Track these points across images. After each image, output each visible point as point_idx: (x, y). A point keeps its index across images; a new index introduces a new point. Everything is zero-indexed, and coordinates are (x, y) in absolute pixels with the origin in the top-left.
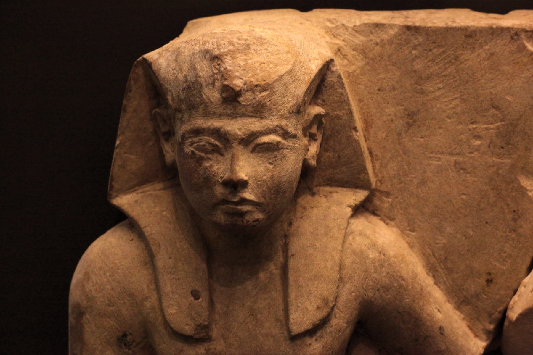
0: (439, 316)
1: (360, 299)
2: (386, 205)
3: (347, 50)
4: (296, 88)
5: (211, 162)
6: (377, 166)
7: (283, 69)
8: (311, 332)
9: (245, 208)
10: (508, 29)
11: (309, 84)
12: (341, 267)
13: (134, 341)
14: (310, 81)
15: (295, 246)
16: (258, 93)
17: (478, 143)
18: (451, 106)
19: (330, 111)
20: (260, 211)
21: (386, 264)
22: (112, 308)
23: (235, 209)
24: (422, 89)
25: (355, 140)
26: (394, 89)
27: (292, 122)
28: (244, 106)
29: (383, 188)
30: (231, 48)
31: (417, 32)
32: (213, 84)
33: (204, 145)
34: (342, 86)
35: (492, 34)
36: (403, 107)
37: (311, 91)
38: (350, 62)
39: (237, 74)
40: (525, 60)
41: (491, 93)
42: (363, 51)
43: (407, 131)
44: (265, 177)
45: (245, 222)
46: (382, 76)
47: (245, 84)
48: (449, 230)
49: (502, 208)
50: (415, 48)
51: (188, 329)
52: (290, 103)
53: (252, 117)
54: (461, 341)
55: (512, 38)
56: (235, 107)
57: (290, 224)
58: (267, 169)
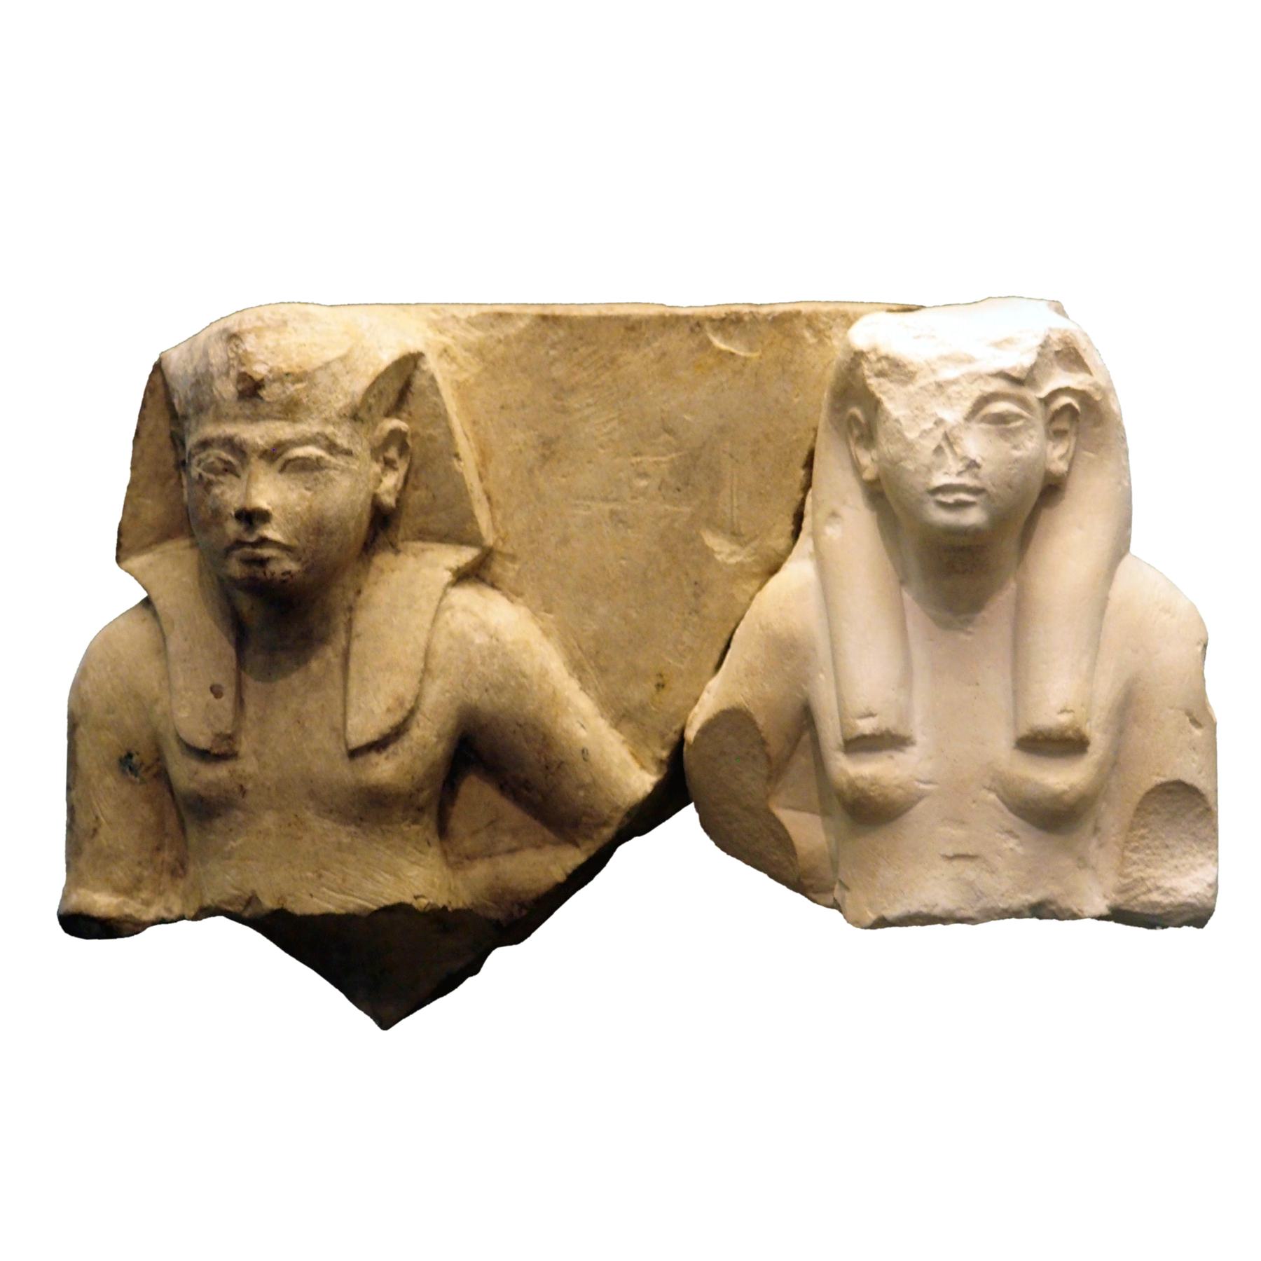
0: (582, 733)
1: (458, 703)
2: (511, 574)
3: (457, 351)
4: (351, 381)
5: (223, 488)
6: (499, 517)
7: (331, 354)
8: (380, 745)
9: (266, 552)
11: (373, 378)
12: (428, 654)
13: (142, 764)
14: (377, 375)
15: (363, 621)
16: (289, 385)
17: (643, 483)
18: (605, 430)
19: (420, 430)
20: (292, 560)
21: (499, 654)
22: (112, 716)
23: (253, 554)
24: (563, 406)
25: (456, 472)
26: (523, 406)
27: (344, 431)
28: (269, 403)
29: (507, 549)
30: (259, 324)
31: (556, 324)
32: (227, 374)
33: (213, 463)
34: (437, 392)
35: (664, 325)
36: (536, 433)
37: (381, 393)
38: (461, 367)
39: (261, 358)
40: (711, 361)
41: (662, 411)
42: (479, 352)
43: (541, 468)
44: (298, 509)
45: (268, 574)
46: (506, 387)
47: (270, 371)
48: (602, 610)
49: (678, 578)
50: (553, 346)
51: (203, 741)
52: (340, 402)
53: (280, 419)
54: (616, 772)
55: (692, 330)
56: (255, 406)
57: (359, 592)
58: (303, 498)
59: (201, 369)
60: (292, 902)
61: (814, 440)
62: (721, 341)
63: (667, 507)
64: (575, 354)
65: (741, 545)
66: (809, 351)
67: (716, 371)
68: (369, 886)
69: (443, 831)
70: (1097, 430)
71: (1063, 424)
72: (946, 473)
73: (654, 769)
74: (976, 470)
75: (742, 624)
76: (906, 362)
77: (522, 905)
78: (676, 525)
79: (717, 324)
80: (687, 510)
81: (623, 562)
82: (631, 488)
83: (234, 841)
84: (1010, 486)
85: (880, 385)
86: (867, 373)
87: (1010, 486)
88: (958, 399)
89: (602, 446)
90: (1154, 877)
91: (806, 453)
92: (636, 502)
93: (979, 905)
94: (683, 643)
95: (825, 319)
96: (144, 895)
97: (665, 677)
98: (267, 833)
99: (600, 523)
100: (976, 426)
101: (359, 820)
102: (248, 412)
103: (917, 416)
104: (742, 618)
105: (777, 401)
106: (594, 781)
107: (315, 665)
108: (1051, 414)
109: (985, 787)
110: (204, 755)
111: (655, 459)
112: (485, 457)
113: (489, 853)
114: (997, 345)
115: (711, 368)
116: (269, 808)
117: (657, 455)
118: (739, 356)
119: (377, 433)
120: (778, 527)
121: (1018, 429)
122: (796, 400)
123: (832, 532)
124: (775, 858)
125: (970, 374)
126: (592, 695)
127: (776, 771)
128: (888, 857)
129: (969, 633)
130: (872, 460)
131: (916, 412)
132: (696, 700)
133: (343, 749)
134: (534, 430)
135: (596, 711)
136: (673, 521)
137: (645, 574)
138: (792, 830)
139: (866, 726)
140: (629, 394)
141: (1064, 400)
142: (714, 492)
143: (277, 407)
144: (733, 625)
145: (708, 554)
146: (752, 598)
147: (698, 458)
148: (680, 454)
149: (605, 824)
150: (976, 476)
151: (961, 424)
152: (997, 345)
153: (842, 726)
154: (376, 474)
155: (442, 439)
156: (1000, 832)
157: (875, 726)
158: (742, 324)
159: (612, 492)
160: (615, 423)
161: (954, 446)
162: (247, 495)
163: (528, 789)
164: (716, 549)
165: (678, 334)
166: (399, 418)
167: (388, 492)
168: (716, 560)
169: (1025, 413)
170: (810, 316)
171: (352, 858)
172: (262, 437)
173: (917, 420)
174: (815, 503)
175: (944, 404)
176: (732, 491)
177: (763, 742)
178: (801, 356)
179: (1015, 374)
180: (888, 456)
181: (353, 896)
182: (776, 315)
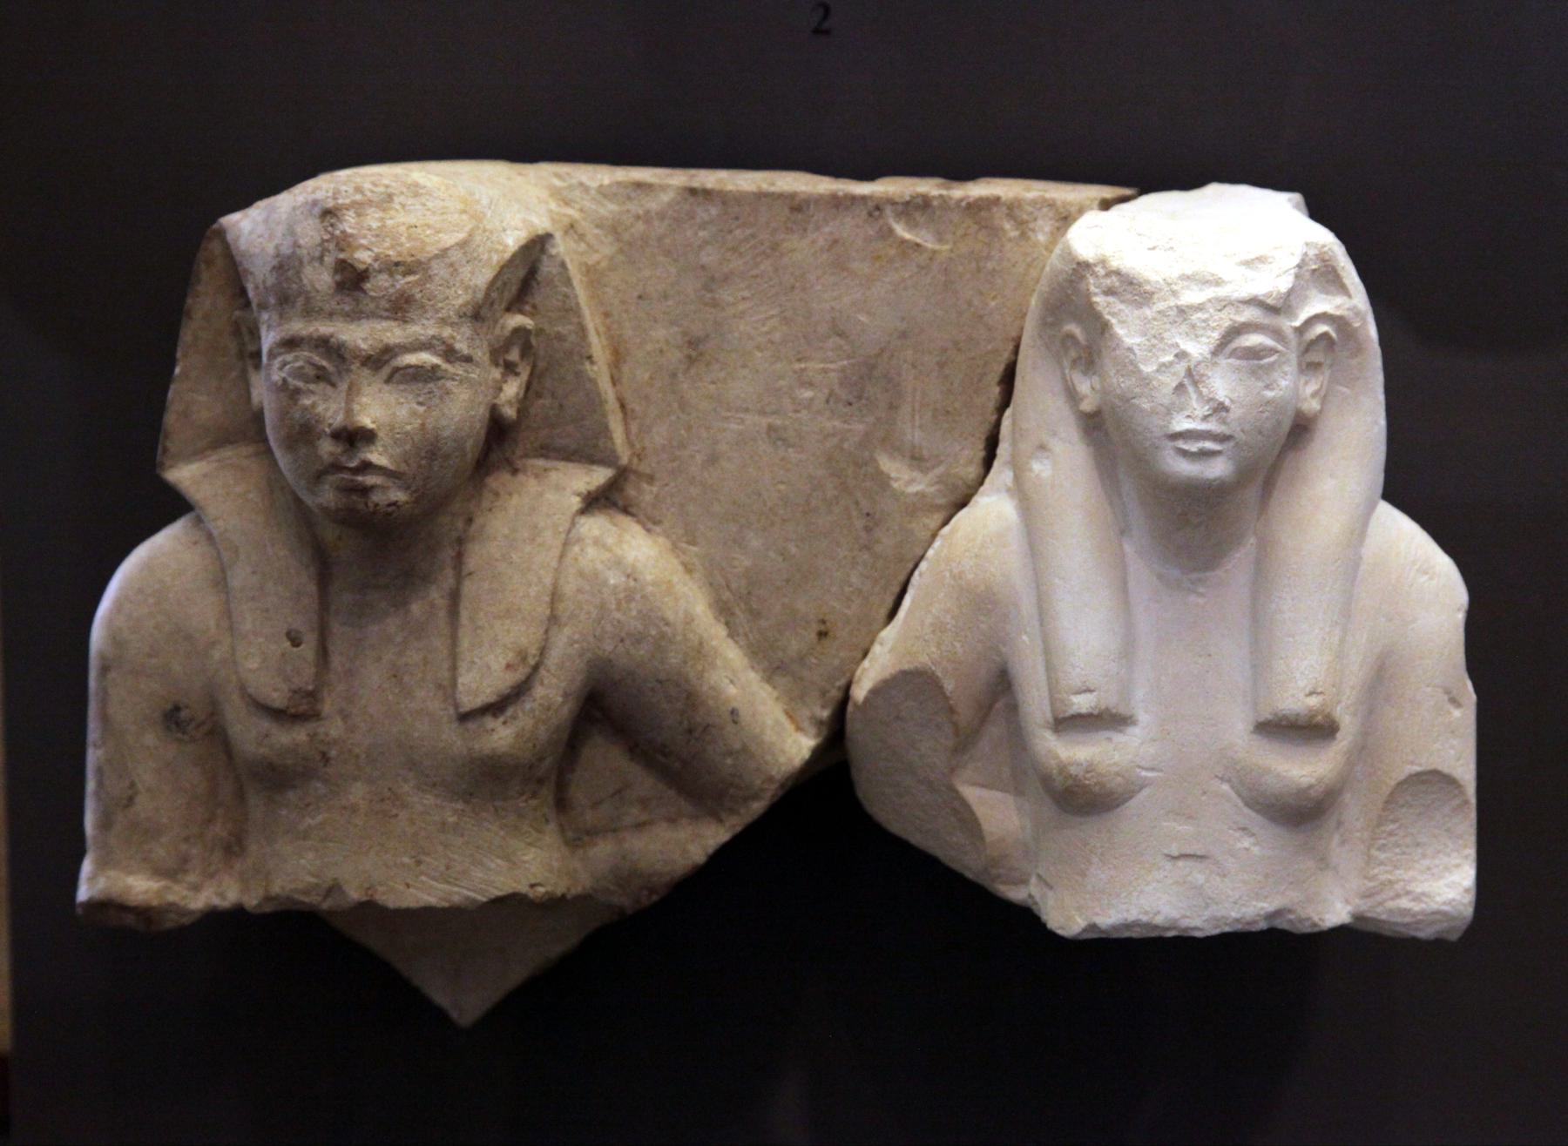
0: (732, 691)
1: (589, 655)
2: (648, 498)
3: (585, 226)
4: (472, 273)
6: (634, 428)
7: (449, 239)
8: (496, 708)
9: (370, 480)
10: (864, 198)
11: (498, 269)
12: (555, 596)
14: (502, 264)
15: (475, 557)
16: (399, 277)
17: (808, 394)
18: (765, 329)
19: (546, 327)
21: (638, 597)
22: (154, 661)
23: (352, 481)
25: (590, 380)
26: (666, 297)
28: (373, 298)
29: (644, 468)
30: (358, 197)
31: (707, 199)
32: (321, 259)
33: (301, 368)
34: (568, 282)
37: (505, 284)
39: (364, 242)
41: (832, 308)
42: (614, 229)
43: (687, 370)
45: (370, 504)
46: (647, 273)
47: (376, 260)
48: (755, 542)
50: (703, 226)
51: (278, 698)
52: (460, 298)
53: (387, 318)
54: (769, 736)
55: (870, 214)
56: (357, 301)
57: (470, 521)
58: (414, 414)
59: (286, 250)
60: (384, 894)
62: (904, 230)
63: (837, 423)
64: (729, 237)
65: (922, 471)
68: (478, 874)
69: (562, 804)
72: (1189, 416)
73: (813, 730)
74: (1224, 414)
75: (923, 566)
76: (1141, 280)
77: (652, 891)
78: (846, 446)
80: (860, 427)
81: (782, 487)
83: (313, 818)
84: (1260, 432)
85: (1109, 304)
86: (1092, 289)
87: (1260, 432)
88: (1204, 328)
89: (758, 348)
92: (799, 415)
93: (1207, 914)
96: (192, 878)
97: (828, 624)
98: (354, 809)
100: (1223, 362)
101: (467, 796)
102: (347, 308)
103: (1154, 346)
104: (922, 557)
105: (970, 304)
106: (745, 749)
107: (416, 608)
109: (1216, 776)
110: (279, 715)
111: (822, 366)
112: (618, 357)
113: (611, 829)
114: (1248, 264)
115: (891, 261)
116: (355, 779)
118: (926, 249)
119: (497, 331)
121: (1271, 365)
122: (993, 304)
123: (1040, 468)
124: (955, 839)
125: (1219, 300)
127: (964, 742)
129: (1202, 595)
130: (1093, 388)
131: (1154, 341)
132: (865, 654)
133: (452, 711)
134: (678, 326)
135: (746, 661)
136: (842, 441)
138: (980, 811)
139: (1082, 703)
140: (793, 288)
141: (1321, 328)
142: (893, 407)
143: (384, 304)
144: (911, 566)
145: (883, 481)
146: (934, 536)
148: (852, 361)
149: (756, 797)
150: (1224, 422)
151: (1207, 359)
154: (495, 380)
155: (572, 338)
156: (1235, 830)
160: (774, 322)
162: (349, 412)
163: (665, 755)
166: (521, 312)
167: (510, 403)
168: (889, 486)
169: (1280, 347)
170: (1012, 204)
171: (459, 841)
172: (364, 340)
173: (1154, 350)
174: (1014, 423)
175: (1187, 333)
177: (952, 710)
178: (1001, 251)
179: (1269, 301)
181: (456, 885)
182: (971, 200)
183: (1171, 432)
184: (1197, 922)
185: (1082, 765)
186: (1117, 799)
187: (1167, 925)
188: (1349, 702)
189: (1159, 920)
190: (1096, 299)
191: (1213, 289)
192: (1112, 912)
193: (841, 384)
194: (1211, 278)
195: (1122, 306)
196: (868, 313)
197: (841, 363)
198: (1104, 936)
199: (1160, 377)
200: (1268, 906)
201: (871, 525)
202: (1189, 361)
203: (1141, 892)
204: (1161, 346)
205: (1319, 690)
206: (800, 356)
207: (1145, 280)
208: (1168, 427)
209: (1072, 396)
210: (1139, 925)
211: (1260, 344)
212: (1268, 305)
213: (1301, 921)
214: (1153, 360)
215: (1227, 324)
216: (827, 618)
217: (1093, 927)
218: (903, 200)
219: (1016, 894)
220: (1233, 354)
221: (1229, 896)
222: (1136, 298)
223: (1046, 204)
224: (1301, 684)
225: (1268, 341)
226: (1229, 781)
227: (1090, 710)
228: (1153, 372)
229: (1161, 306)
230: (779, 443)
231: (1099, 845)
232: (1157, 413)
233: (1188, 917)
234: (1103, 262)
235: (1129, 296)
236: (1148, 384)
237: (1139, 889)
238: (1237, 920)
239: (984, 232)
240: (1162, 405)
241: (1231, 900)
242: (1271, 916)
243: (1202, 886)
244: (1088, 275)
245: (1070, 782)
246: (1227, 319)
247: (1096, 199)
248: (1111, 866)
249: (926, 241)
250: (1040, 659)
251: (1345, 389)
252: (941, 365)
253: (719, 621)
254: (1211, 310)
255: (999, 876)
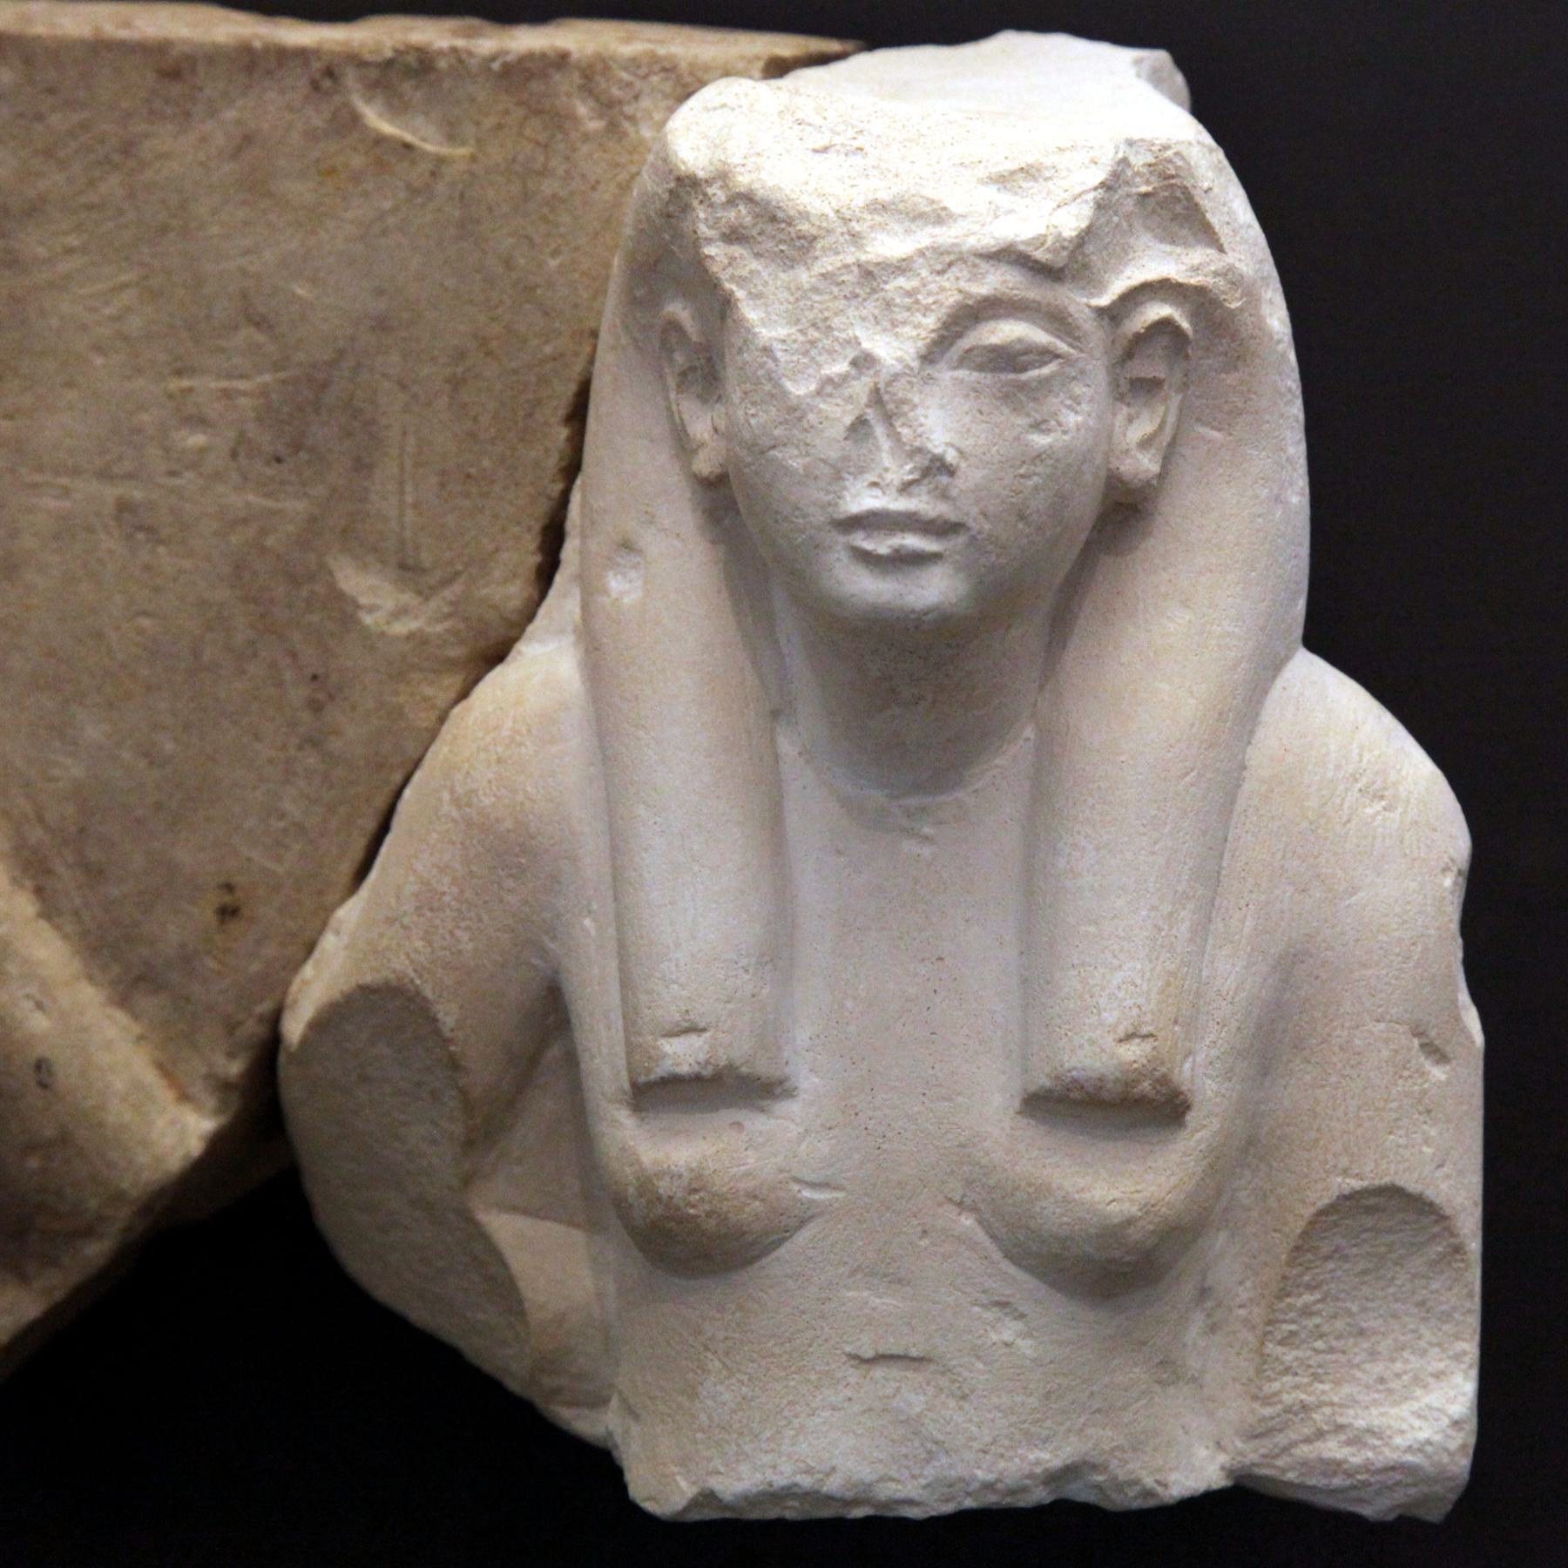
0: (39, 1023)
17: (197, 439)
18: (107, 311)
40: (357, 161)
41: (243, 272)
48: (93, 732)
49: (273, 665)
54: (118, 1113)
55: (315, 86)
61: (591, 361)
62: (380, 115)
63: (251, 498)
64: (39, 127)
65: (419, 593)
66: (585, 149)
67: (369, 185)
70: (1231, 379)
71: (1149, 366)
72: (874, 484)
73: (211, 1102)
74: (944, 479)
75: (417, 777)
76: (792, 213)
78: (270, 541)
79: (374, 74)
81: (145, 622)
82: (167, 450)
84: (1022, 517)
85: (732, 260)
86: (703, 229)
87: (1022, 517)
88: (909, 309)
89: (99, 349)
90: (1332, 1404)
91: (572, 388)
92: (178, 482)
93: (930, 1472)
94: (282, 816)
95: (625, 76)
97: (239, 894)
99: (90, 530)
100: (946, 375)
103: (813, 343)
104: (417, 764)
105: (508, 263)
106: (64, 1139)
108: (1125, 342)
109: (950, 1200)
111: (224, 384)
114: (1003, 180)
115: (356, 178)
117: (229, 376)
118: (424, 154)
120: (505, 556)
121: (1045, 382)
122: (553, 263)
123: (622, 587)
124: (480, 1316)
125: (938, 251)
126: (69, 928)
128: (727, 1353)
129: (926, 839)
130: (716, 430)
131: (816, 334)
132: (310, 948)
135: (76, 966)
136: (263, 532)
137: (196, 653)
138: (520, 1262)
139: (681, 1055)
140: (164, 230)
141: (1157, 311)
142: (361, 466)
144: (397, 777)
145: (343, 610)
146: (442, 719)
147: (324, 386)
148: (282, 375)
149: (89, 1232)
150: (944, 495)
151: (911, 369)
152: (1003, 180)
153: (631, 1049)
156: (984, 1306)
157: (702, 1057)
158: (433, 77)
159: (120, 458)
161: (897, 424)
164: (363, 600)
165: (282, 92)
168: (359, 622)
169: (1062, 347)
170: (591, 66)
173: (813, 352)
174: (584, 504)
175: (876, 318)
176: (402, 468)
177: (454, 1064)
178: (567, 158)
179: (1040, 255)
180: (747, 436)
182: (509, 58)
183: (842, 516)
184: (910, 1490)
185: (680, 1176)
186: (753, 1243)
187: (849, 1495)
188: (1213, 1052)
189: (833, 1485)
190: (710, 250)
191: (930, 229)
192: (744, 1468)
193: (259, 420)
194: (928, 209)
195: (755, 265)
196: (314, 281)
197: (259, 379)
198: (728, 1515)
199: (822, 406)
200: (1050, 1457)
201: (321, 696)
202: (877, 373)
203: (802, 1427)
204: (827, 342)
205: (1145, 1030)
206: (179, 364)
207: (800, 213)
208: (836, 505)
209: (683, 445)
210: (795, 1495)
211: (1020, 340)
212: (1036, 262)
213: (1120, 1486)
214: (810, 371)
215: (952, 299)
216: (239, 880)
217: (708, 1497)
218: (379, 59)
219: (587, 1424)
220: (965, 360)
221: (971, 1439)
222: (782, 247)
223: (656, 68)
224: (1110, 1017)
225: (1038, 335)
226: (974, 1209)
227: (696, 1068)
228: (806, 396)
229: (828, 263)
230: (141, 536)
231: (721, 1335)
232: (816, 478)
233: (893, 1480)
234: (723, 176)
235: (770, 245)
236: (800, 419)
237: (796, 1422)
238: (989, 1486)
239: (535, 122)
240: (824, 461)
241: (976, 1445)
242: (1053, 1478)
243: (919, 1416)
244: (695, 203)
245: (659, 1210)
246: (952, 290)
247: (757, 58)
248: (745, 1378)
249: (424, 140)
250: (613, 966)
251: (1216, 434)
252: (456, 383)
253: (22, 886)
254: (924, 273)
255: (557, 1391)
